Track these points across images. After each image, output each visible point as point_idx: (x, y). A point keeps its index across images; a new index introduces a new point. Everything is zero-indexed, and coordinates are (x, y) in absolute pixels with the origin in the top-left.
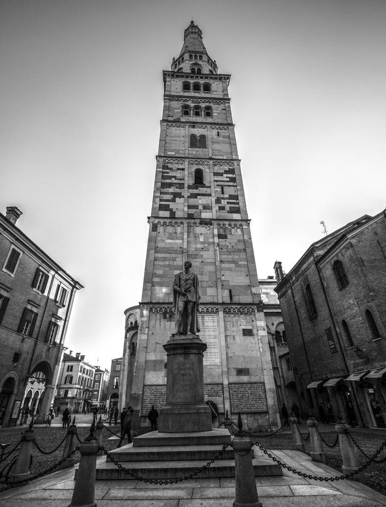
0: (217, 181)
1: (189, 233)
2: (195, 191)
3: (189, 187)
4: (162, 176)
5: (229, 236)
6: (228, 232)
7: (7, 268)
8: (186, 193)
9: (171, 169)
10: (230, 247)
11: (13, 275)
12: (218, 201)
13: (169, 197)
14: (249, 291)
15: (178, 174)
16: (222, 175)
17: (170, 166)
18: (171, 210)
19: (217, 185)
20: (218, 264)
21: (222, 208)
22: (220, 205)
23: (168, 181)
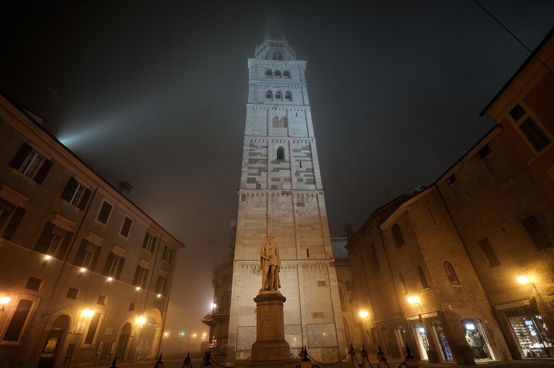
0: (296, 157)
1: (273, 201)
2: (277, 166)
3: (273, 162)
4: (250, 153)
5: (306, 204)
6: (305, 201)
7: (122, 233)
8: (271, 167)
9: (255, 147)
10: (307, 213)
11: (127, 239)
12: (297, 173)
13: (256, 171)
14: (323, 250)
15: (263, 151)
16: (300, 151)
17: (255, 144)
18: (257, 183)
19: (296, 160)
20: (297, 227)
21: (300, 180)
22: (299, 177)
23: (255, 157)
